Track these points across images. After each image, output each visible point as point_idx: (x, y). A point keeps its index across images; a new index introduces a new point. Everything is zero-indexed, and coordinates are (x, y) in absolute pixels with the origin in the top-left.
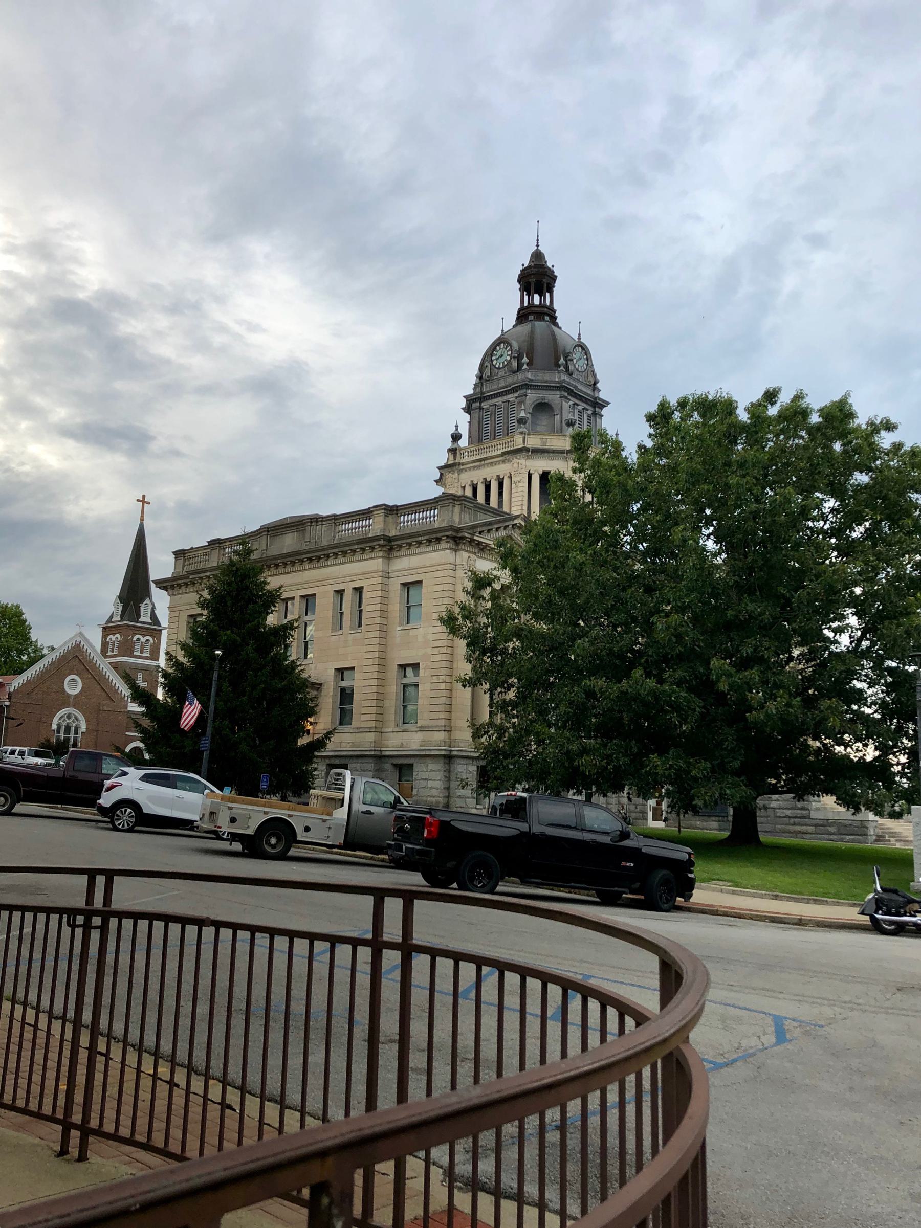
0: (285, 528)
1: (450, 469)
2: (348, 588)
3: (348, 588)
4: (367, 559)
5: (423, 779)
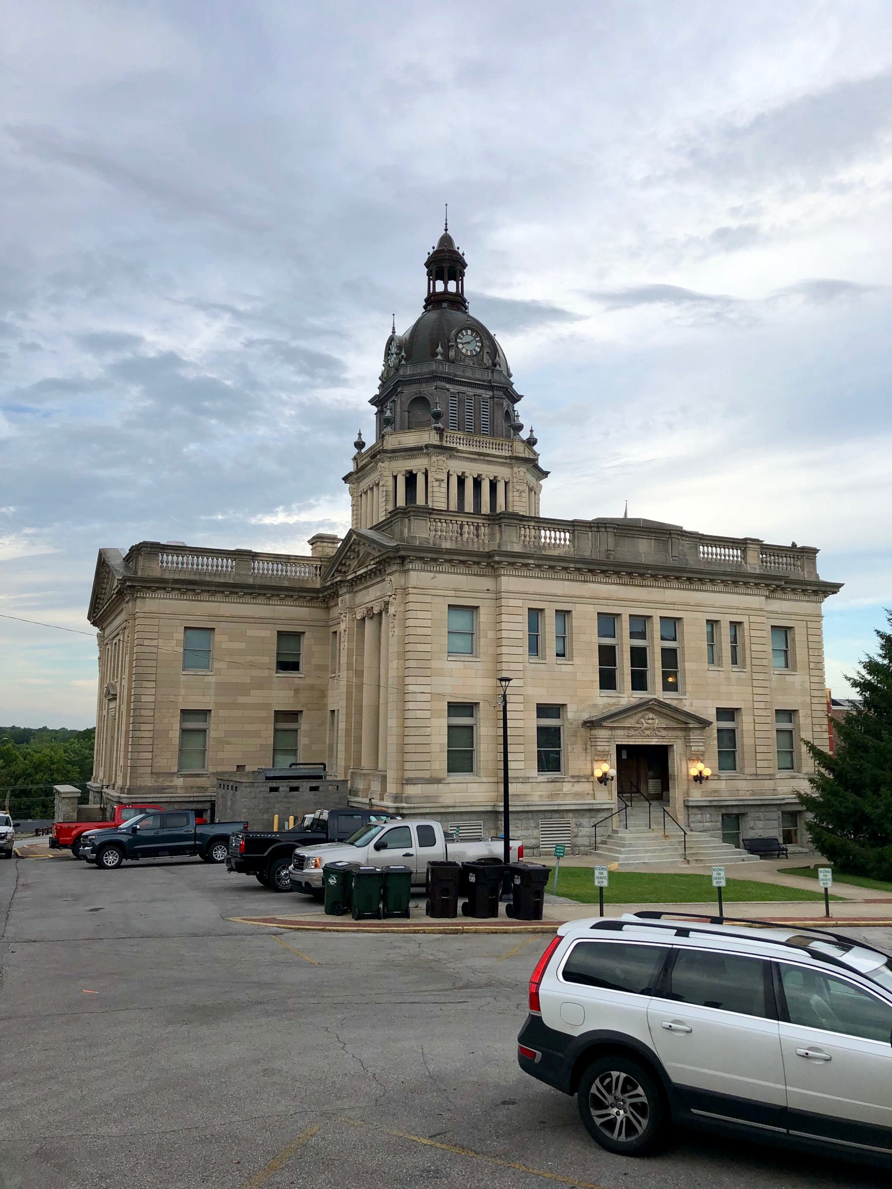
0: (650, 532)
1: (439, 450)
2: (725, 621)
3: (725, 621)
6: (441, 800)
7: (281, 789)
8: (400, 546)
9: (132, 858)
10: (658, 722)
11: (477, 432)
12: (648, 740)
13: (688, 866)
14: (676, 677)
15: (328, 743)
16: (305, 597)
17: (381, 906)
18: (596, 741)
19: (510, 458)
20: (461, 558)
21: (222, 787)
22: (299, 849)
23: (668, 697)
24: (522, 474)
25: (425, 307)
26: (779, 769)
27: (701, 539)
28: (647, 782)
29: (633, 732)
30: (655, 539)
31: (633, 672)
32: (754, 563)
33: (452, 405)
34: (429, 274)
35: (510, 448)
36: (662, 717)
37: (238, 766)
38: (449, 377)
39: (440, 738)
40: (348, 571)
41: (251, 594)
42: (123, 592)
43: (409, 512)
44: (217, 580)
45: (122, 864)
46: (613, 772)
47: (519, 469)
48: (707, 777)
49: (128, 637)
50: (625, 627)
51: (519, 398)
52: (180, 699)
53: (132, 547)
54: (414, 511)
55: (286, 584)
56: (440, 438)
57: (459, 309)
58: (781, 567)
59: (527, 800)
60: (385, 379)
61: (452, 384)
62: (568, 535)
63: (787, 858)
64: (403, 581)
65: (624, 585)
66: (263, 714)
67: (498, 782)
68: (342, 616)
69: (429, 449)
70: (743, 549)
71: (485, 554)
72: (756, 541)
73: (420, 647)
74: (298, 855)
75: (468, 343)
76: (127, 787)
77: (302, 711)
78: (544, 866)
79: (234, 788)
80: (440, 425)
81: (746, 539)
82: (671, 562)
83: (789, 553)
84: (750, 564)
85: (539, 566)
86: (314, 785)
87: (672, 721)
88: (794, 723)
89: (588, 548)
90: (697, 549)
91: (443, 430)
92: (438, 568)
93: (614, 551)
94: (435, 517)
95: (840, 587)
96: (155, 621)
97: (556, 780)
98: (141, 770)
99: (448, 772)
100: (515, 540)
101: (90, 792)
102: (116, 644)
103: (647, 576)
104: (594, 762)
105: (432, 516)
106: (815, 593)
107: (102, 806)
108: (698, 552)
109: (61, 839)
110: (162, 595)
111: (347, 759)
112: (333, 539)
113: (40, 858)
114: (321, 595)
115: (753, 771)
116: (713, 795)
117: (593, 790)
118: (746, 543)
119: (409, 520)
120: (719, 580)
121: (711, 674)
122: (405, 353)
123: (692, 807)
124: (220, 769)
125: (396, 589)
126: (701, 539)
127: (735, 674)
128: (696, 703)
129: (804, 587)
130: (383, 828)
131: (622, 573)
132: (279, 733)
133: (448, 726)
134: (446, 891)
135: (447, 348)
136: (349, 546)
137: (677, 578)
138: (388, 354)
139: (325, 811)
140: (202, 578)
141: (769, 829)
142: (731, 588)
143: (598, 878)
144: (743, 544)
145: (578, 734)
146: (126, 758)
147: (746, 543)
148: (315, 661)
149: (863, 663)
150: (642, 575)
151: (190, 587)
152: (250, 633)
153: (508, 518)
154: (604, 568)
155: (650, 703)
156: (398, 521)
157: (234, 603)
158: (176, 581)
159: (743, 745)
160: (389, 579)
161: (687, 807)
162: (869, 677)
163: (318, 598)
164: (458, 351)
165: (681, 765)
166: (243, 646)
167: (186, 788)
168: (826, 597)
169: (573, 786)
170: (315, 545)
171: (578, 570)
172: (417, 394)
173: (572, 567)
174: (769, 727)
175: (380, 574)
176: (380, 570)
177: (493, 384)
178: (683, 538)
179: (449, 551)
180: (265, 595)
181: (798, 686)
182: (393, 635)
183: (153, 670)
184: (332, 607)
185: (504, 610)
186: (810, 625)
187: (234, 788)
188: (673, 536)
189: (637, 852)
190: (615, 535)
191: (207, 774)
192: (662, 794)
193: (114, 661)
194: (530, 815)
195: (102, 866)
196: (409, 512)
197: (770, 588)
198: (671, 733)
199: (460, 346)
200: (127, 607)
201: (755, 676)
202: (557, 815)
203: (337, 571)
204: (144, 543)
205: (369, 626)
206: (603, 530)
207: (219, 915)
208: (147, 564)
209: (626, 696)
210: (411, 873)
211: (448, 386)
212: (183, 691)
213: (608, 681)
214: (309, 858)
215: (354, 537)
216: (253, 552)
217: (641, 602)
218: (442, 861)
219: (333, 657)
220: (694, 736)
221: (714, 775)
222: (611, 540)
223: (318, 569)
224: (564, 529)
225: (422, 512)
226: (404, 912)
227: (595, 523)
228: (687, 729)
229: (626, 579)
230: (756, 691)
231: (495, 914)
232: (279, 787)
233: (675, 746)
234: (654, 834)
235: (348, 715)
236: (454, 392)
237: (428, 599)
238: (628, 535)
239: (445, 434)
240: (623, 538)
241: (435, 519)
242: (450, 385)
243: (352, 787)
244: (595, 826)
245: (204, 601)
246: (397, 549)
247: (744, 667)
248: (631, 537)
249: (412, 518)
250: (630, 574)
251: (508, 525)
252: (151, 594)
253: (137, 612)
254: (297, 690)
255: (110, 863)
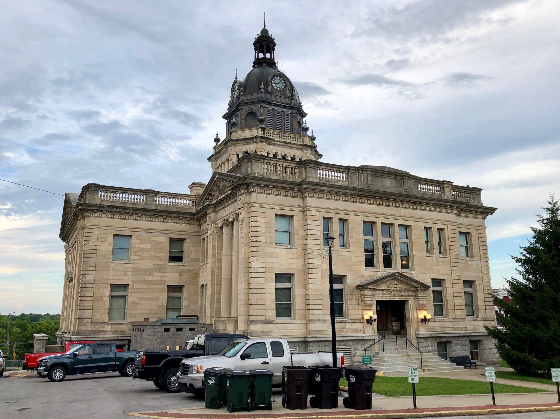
0: (391, 174)
1: (262, 140)
2: (435, 227)
3: (435, 227)
4: (447, 213)
5: (489, 349)
6: (272, 334)
7: (171, 330)
8: (247, 176)
9: (72, 374)
10: (400, 286)
11: (283, 131)
12: (394, 297)
13: (424, 373)
14: (402, 264)
15: (199, 304)
16: (186, 218)
17: (249, 401)
18: (365, 298)
19: (303, 145)
20: (283, 185)
21: (135, 330)
22: (183, 360)
23: (404, 271)
24: (309, 154)
25: (253, 67)
26: (467, 315)
27: (419, 180)
28: (392, 325)
29: (385, 293)
30: (394, 179)
31: (384, 257)
32: (448, 194)
33: (269, 116)
34: (255, 49)
35: (302, 141)
36: (402, 284)
37: (145, 319)
38: (268, 101)
39: (271, 296)
40: (213, 199)
41: (154, 215)
42: (77, 213)
43: (252, 157)
44: (134, 206)
45: (65, 379)
46: (375, 317)
47: (307, 152)
48: (429, 319)
49: (79, 240)
50: (379, 228)
51: (306, 114)
52: (110, 277)
53: (83, 187)
54: (254, 157)
55: (175, 210)
56: (263, 133)
57: (272, 67)
58: (463, 198)
59: (325, 334)
60: (231, 105)
61: (269, 105)
62: (344, 175)
63: (476, 368)
64: (247, 199)
65: (378, 205)
66: (161, 287)
67: (306, 323)
68: (209, 226)
69: (258, 138)
70: (442, 187)
71: (297, 183)
72: (450, 183)
73: (258, 239)
74: (184, 364)
75: (278, 83)
76: (76, 331)
77: (184, 286)
78: (371, 368)
79: (142, 330)
80: (263, 126)
81: (444, 181)
82: (403, 192)
83: (466, 191)
84: (446, 195)
85: (329, 192)
86: (192, 327)
87: (407, 286)
88: (473, 289)
89: (356, 182)
90: (417, 186)
91: (265, 129)
92: (269, 191)
93: (372, 184)
94: (267, 161)
95: (496, 210)
96: (96, 231)
97: (341, 321)
98: (85, 321)
99: (276, 317)
100: (314, 176)
101: (58, 338)
102: (74, 249)
103: (391, 199)
104: (364, 310)
105: (265, 161)
106: (482, 213)
107: (62, 345)
108: (417, 188)
109: (29, 364)
110: (100, 215)
111: (212, 312)
112: (202, 185)
113: (19, 377)
114: (196, 217)
115: (453, 316)
116: (432, 330)
117: (363, 328)
118: (444, 184)
119: (251, 163)
120: (431, 203)
121: (428, 259)
122: (243, 88)
123: (421, 338)
124: (134, 320)
125: (244, 204)
126: (419, 180)
127: (441, 259)
128: (420, 275)
129: (476, 210)
130: (246, 343)
131: (377, 198)
132: (170, 299)
133: (276, 288)
134: (299, 388)
135: (266, 86)
136: (214, 182)
137: (408, 202)
138: (233, 90)
139: (202, 335)
140: (125, 205)
141: (464, 351)
142: (437, 209)
143: (411, 376)
144: (443, 184)
145: (354, 294)
146: (76, 313)
147: (444, 184)
148: (192, 256)
149: (522, 248)
150: (388, 199)
151: (118, 210)
152: (153, 238)
153: (310, 163)
154: (367, 194)
155: (396, 275)
156: (244, 164)
157: (144, 220)
158: (109, 207)
159: (447, 301)
160: (239, 198)
161: (418, 338)
162: (528, 256)
163: (194, 219)
164: (273, 87)
165: (413, 313)
166: (149, 246)
167: (113, 332)
168: (487, 216)
169: (351, 325)
170: (192, 189)
171: (352, 195)
172: (250, 110)
173: (348, 193)
174: (461, 290)
175: (233, 197)
176: (233, 195)
177: (291, 106)
178: (410, 179)
179: (276, 181)
180: (162, 216)
181: (474, 267)
182: (242, 233)
183: (94, 260)
184: (202, 224)
185: (309, 217)
186: (480, 232)
187: (142, 330)
188: (404, 177)
189: (393, 365)
190: (372, 176)
191: (126, 323)
192: (400, 331)
193: (73, 259)
194: (327, 343)
195: (52, 380)
196: (252, 157)
197: (459, 209)
198: (407, 293)
199: (274, 85)
200: (80, 223)
201: (452, 260)
202: (343, 343)
203: (207, 199)
204: (90, 184)
205: (226, 230)
206: (365, 172)
207: (122, 411)
208: (92, 197)
209: (380, 271)
210: (272, 374)
211: (267, 106)
212: (112, 273)
213: (370, 263)
214: (192, 366)
215: (217, 176)
216: (156, 191)
217: (388, 215)
218: (289, 365)
219: (203, 254)
220: (420, 294)
221: (432, 319)
222: (370, 178)
223: (194, 202)
224: (342, 171)
225: (259, 158)
226: (267, 405)
227: (360, 168)
228: (416, 291)
229: (379, 201)
230: (453, 269)
231: (335, 405)
232: (170, 329)
233: (409, 301)
234: (400, 354)
235: (212, 286)
236: (270, 110)
237: (263, 210)
238: (380, 176)
239: (266, 131)
240: (376, 178)
241: (267, 163)
242: (268, 106)
243: (215, 329)
244: (365, 350)
245: (126, 219)
246: (245, 179)
247: (446, 254)
248: (381, 177)
249: (253, 161)
250: (381, 198)
251: (310, 168)
252: (93, 214)
253: (85, 225)
254: (181, 273)
255: (57, 378)
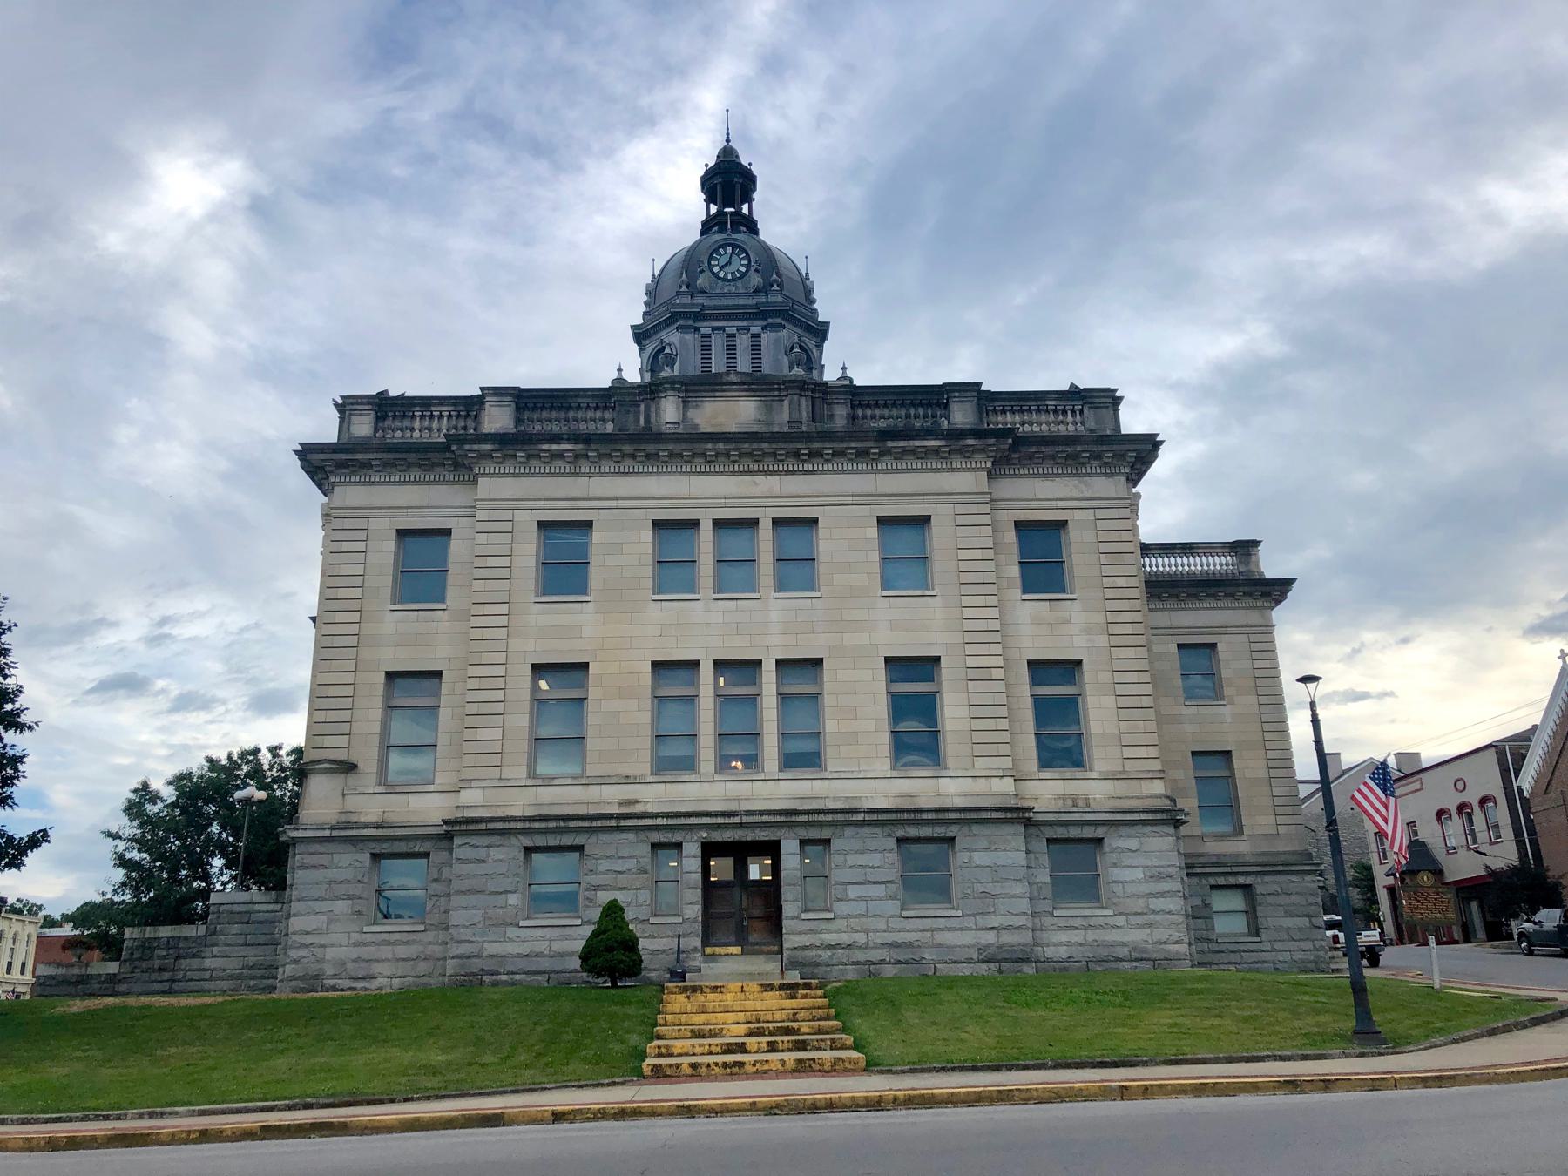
75: (729, 263)
199: (716, 269)
